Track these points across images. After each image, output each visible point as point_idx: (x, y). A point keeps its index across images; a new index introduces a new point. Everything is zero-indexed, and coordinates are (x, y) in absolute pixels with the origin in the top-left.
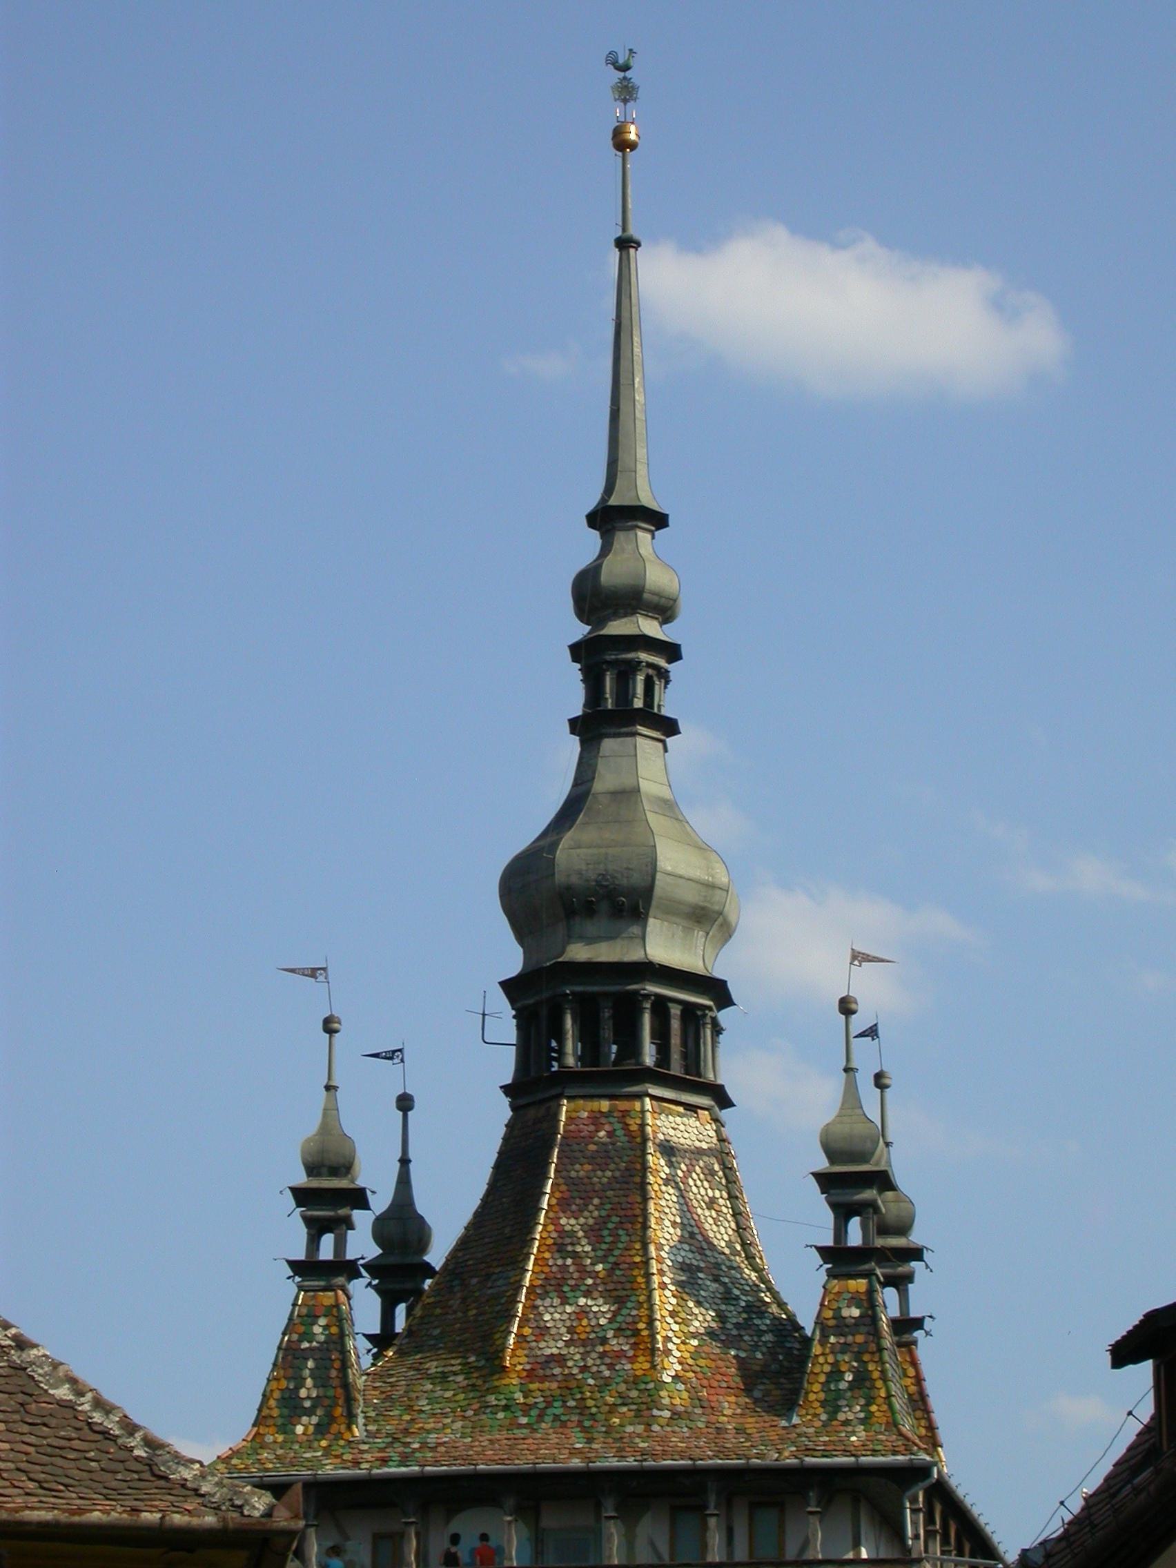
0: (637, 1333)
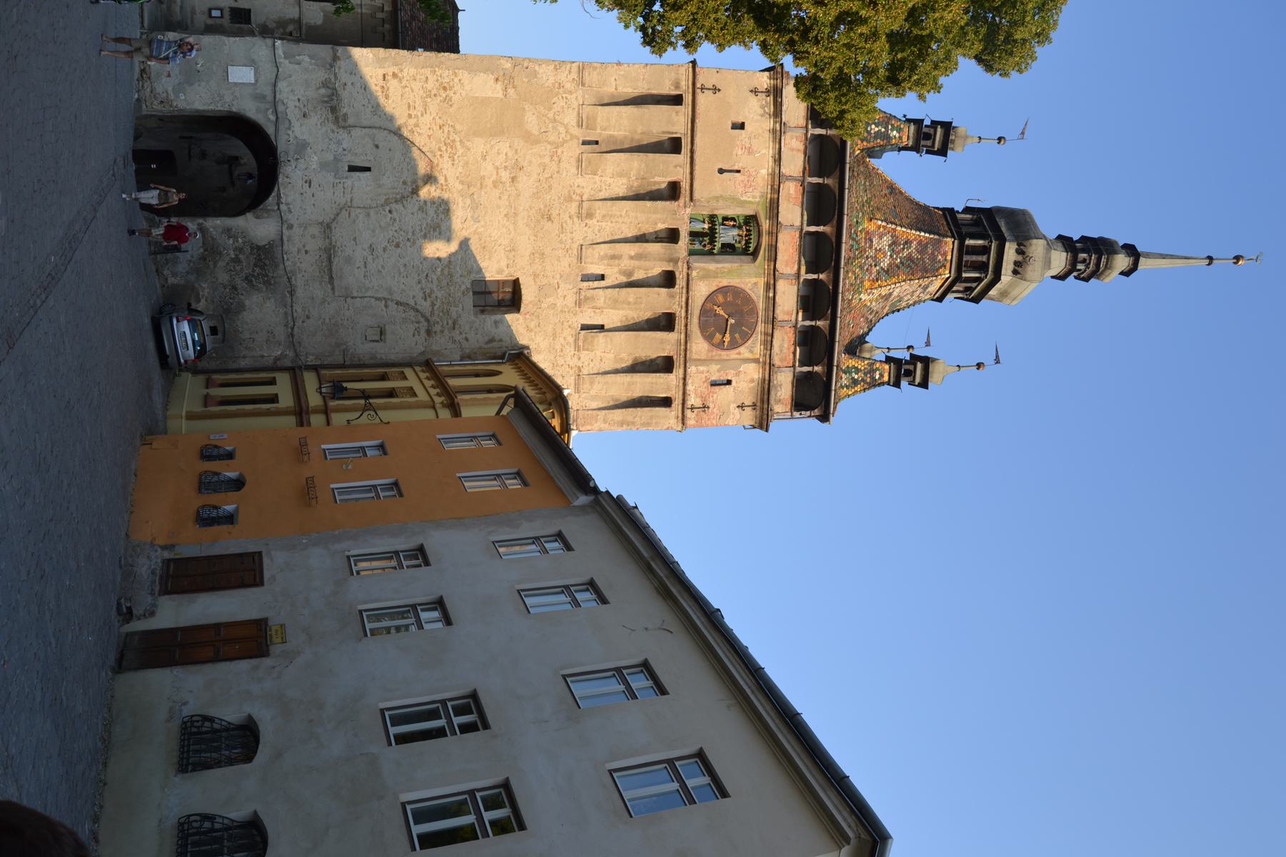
0: (877, 281)
